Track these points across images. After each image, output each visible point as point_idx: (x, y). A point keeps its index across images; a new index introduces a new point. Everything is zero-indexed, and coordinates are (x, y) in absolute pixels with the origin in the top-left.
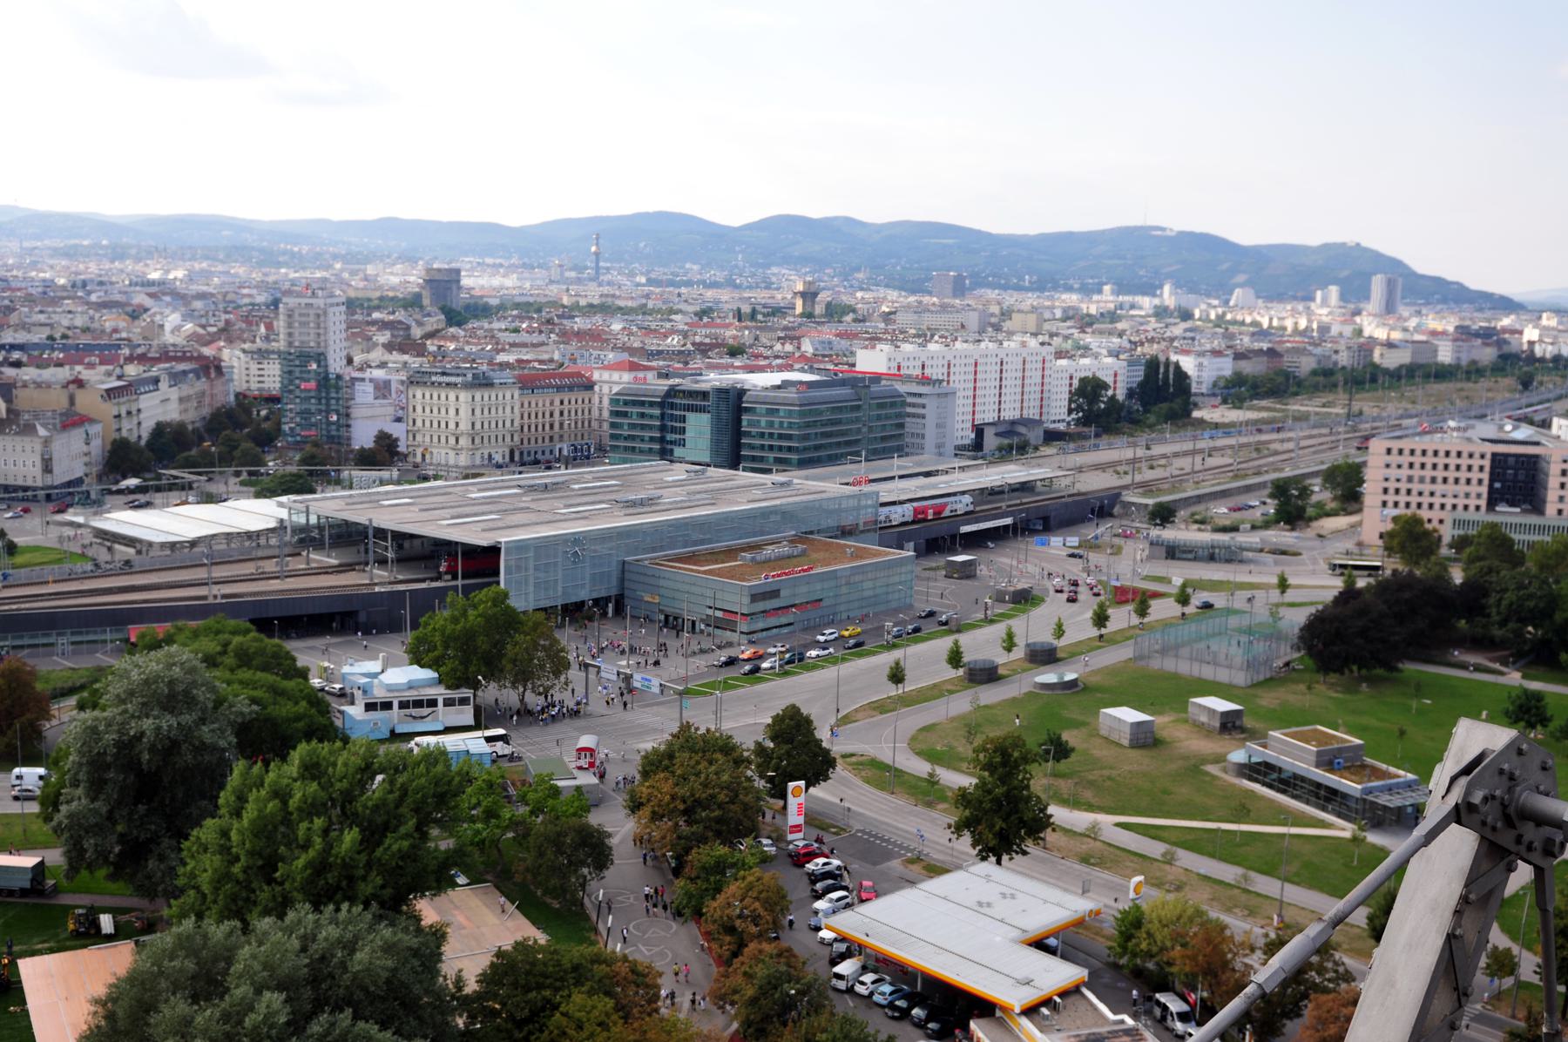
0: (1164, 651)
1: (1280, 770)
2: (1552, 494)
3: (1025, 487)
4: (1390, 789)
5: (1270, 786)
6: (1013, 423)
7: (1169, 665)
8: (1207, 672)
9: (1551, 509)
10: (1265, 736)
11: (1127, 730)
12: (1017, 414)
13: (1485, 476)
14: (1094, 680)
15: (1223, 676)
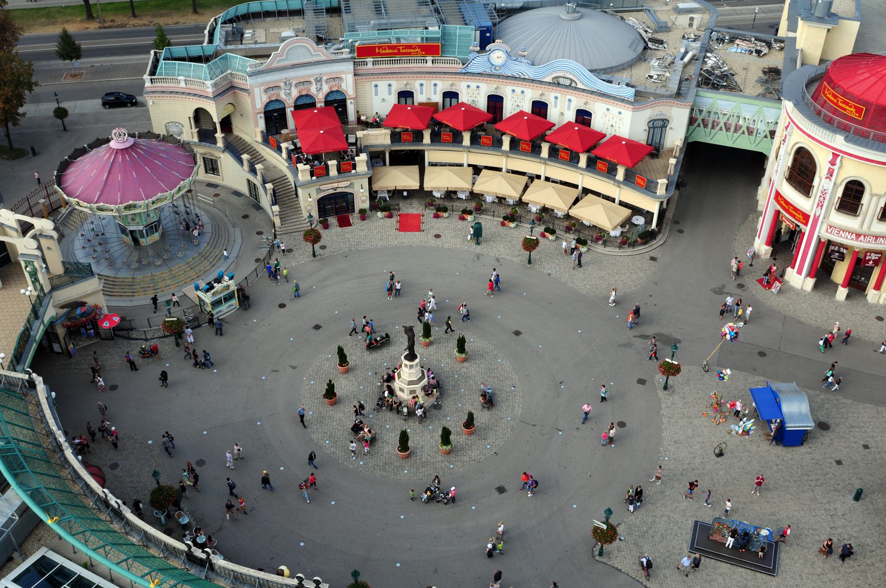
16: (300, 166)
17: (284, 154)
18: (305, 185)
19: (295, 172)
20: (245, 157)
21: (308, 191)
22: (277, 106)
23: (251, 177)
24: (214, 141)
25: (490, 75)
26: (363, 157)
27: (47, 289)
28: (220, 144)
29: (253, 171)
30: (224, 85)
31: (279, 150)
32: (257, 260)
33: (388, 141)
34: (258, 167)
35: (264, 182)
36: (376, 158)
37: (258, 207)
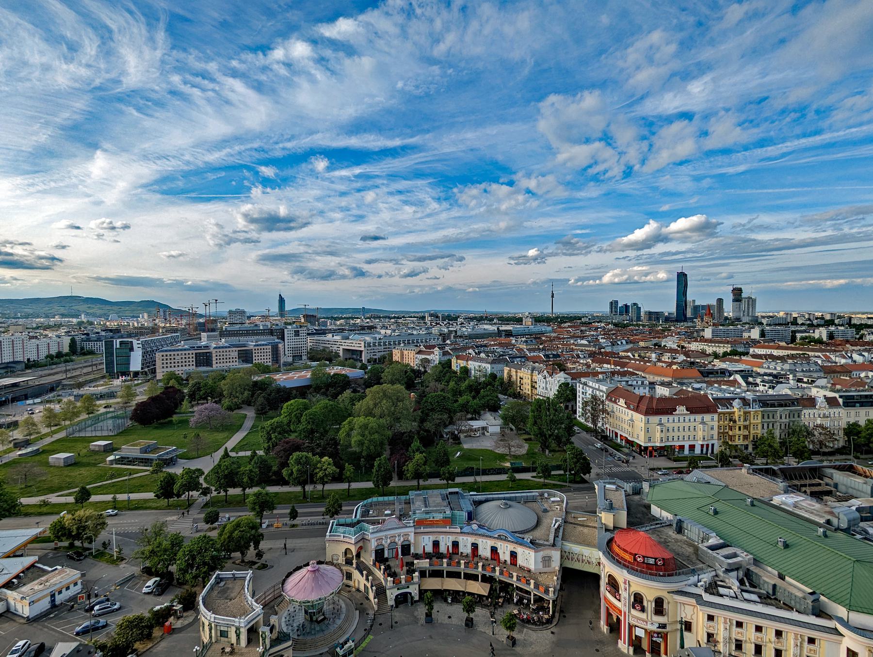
0: (80, 431)
1: (128, 458)
2: (214, 362)
3: (14, 385)
4: (167, 453)
5: (125, 464)
6: (8, 363)
7: (82, 434)
8: (99, 434)
9: (214, 366)
10: (120, 449)
11: (62, 461)
12: (11, 360)
13: (194, 359)
14: (46, 448)
15: (105, 433)
16: (389, 579)
17: (382, 572)
18: (390, 589)
19: (386, 581)
20: (365, 572)
21: (392, 591)
22: (381, 547)
23: (366, 583)
24: (352, 564)
25: (472, 534)
26: (417, 574)
27: (268, 647)
28: (354, 566)
29: (367, 579)
30: (360, 538)
31: (380, 569)
32: (365, 630)
33: (428, 565)
34: (370, 578)
35: (372, 586)
36: (423, 574)
37: (367, 598)
